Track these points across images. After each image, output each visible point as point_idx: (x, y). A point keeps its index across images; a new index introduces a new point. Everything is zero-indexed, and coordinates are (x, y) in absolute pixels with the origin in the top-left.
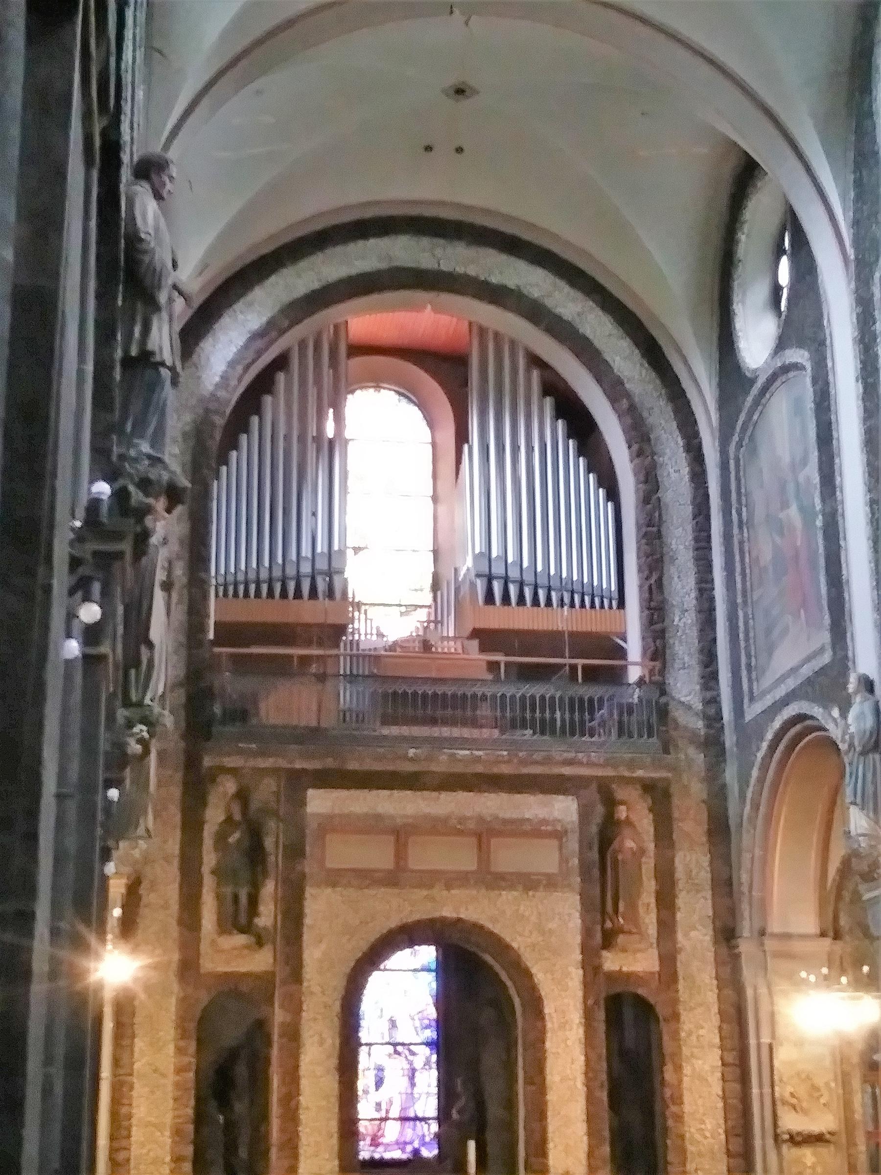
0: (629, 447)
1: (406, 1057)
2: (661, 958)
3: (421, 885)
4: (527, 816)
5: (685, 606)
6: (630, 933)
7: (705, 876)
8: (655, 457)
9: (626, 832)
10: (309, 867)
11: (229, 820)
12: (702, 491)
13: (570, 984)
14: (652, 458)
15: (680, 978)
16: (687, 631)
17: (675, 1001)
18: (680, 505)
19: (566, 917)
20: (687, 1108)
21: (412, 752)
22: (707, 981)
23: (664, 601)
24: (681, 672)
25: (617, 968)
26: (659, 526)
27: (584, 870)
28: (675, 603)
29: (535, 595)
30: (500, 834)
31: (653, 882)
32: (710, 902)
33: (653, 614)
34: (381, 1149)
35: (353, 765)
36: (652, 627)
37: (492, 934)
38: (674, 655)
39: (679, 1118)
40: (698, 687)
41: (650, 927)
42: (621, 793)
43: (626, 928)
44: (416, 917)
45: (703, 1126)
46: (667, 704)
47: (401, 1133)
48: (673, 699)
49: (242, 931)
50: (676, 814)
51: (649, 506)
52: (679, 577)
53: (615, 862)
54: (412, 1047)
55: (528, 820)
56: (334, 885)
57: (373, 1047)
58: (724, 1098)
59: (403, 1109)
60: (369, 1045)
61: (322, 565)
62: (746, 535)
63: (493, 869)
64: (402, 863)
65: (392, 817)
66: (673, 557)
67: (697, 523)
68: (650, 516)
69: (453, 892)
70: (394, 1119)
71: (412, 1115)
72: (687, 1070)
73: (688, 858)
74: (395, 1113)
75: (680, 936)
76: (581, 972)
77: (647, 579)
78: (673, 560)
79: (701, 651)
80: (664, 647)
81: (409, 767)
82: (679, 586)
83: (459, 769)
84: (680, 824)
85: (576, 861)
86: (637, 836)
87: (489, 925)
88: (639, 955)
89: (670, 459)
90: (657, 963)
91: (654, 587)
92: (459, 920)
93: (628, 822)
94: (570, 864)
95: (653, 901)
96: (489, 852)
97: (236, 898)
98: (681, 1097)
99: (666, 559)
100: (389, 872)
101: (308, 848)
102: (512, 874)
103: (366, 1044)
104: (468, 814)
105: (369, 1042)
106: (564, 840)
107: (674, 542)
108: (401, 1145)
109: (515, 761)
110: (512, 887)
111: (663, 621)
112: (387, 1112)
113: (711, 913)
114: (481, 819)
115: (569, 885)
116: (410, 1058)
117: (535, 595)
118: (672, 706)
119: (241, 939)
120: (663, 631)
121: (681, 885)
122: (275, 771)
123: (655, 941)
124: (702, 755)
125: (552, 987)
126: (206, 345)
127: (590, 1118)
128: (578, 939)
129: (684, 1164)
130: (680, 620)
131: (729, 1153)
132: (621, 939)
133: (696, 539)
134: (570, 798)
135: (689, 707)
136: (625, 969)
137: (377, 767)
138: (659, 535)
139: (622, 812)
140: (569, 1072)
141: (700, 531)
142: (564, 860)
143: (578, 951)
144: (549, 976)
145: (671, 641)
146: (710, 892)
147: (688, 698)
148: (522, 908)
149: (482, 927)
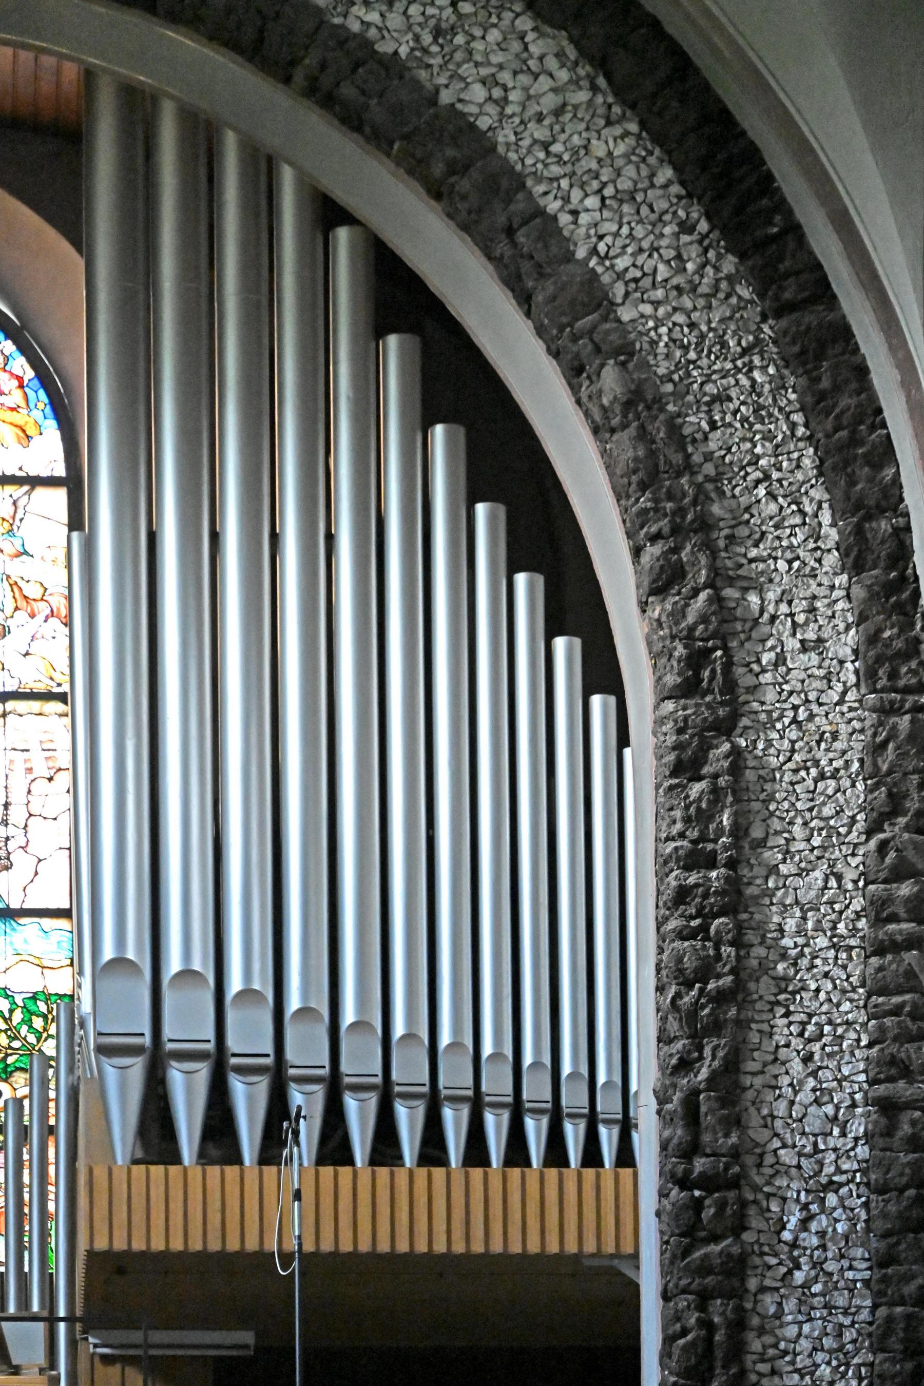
0: (637, 552)
5: (829, 1169)
8: (730, 593)
14: (717, 600)
16: (831, 1266)
18: (822, 776)
28: (787, 1157)
33: (698, 1205)
36: (697, 1254)
51: (696, 789)
52: (807, 1059)
66: (786, 979)
67: (883, 847)
77: (685, 1065)
80: (738, 1325)
82: (805, 1096)
89: (786, 597)
91: (705, 1102)
99: (764, 988)
107: (791, 925)
111: (739, 1227)
130: (804, 1224)
145: (769, 1303)
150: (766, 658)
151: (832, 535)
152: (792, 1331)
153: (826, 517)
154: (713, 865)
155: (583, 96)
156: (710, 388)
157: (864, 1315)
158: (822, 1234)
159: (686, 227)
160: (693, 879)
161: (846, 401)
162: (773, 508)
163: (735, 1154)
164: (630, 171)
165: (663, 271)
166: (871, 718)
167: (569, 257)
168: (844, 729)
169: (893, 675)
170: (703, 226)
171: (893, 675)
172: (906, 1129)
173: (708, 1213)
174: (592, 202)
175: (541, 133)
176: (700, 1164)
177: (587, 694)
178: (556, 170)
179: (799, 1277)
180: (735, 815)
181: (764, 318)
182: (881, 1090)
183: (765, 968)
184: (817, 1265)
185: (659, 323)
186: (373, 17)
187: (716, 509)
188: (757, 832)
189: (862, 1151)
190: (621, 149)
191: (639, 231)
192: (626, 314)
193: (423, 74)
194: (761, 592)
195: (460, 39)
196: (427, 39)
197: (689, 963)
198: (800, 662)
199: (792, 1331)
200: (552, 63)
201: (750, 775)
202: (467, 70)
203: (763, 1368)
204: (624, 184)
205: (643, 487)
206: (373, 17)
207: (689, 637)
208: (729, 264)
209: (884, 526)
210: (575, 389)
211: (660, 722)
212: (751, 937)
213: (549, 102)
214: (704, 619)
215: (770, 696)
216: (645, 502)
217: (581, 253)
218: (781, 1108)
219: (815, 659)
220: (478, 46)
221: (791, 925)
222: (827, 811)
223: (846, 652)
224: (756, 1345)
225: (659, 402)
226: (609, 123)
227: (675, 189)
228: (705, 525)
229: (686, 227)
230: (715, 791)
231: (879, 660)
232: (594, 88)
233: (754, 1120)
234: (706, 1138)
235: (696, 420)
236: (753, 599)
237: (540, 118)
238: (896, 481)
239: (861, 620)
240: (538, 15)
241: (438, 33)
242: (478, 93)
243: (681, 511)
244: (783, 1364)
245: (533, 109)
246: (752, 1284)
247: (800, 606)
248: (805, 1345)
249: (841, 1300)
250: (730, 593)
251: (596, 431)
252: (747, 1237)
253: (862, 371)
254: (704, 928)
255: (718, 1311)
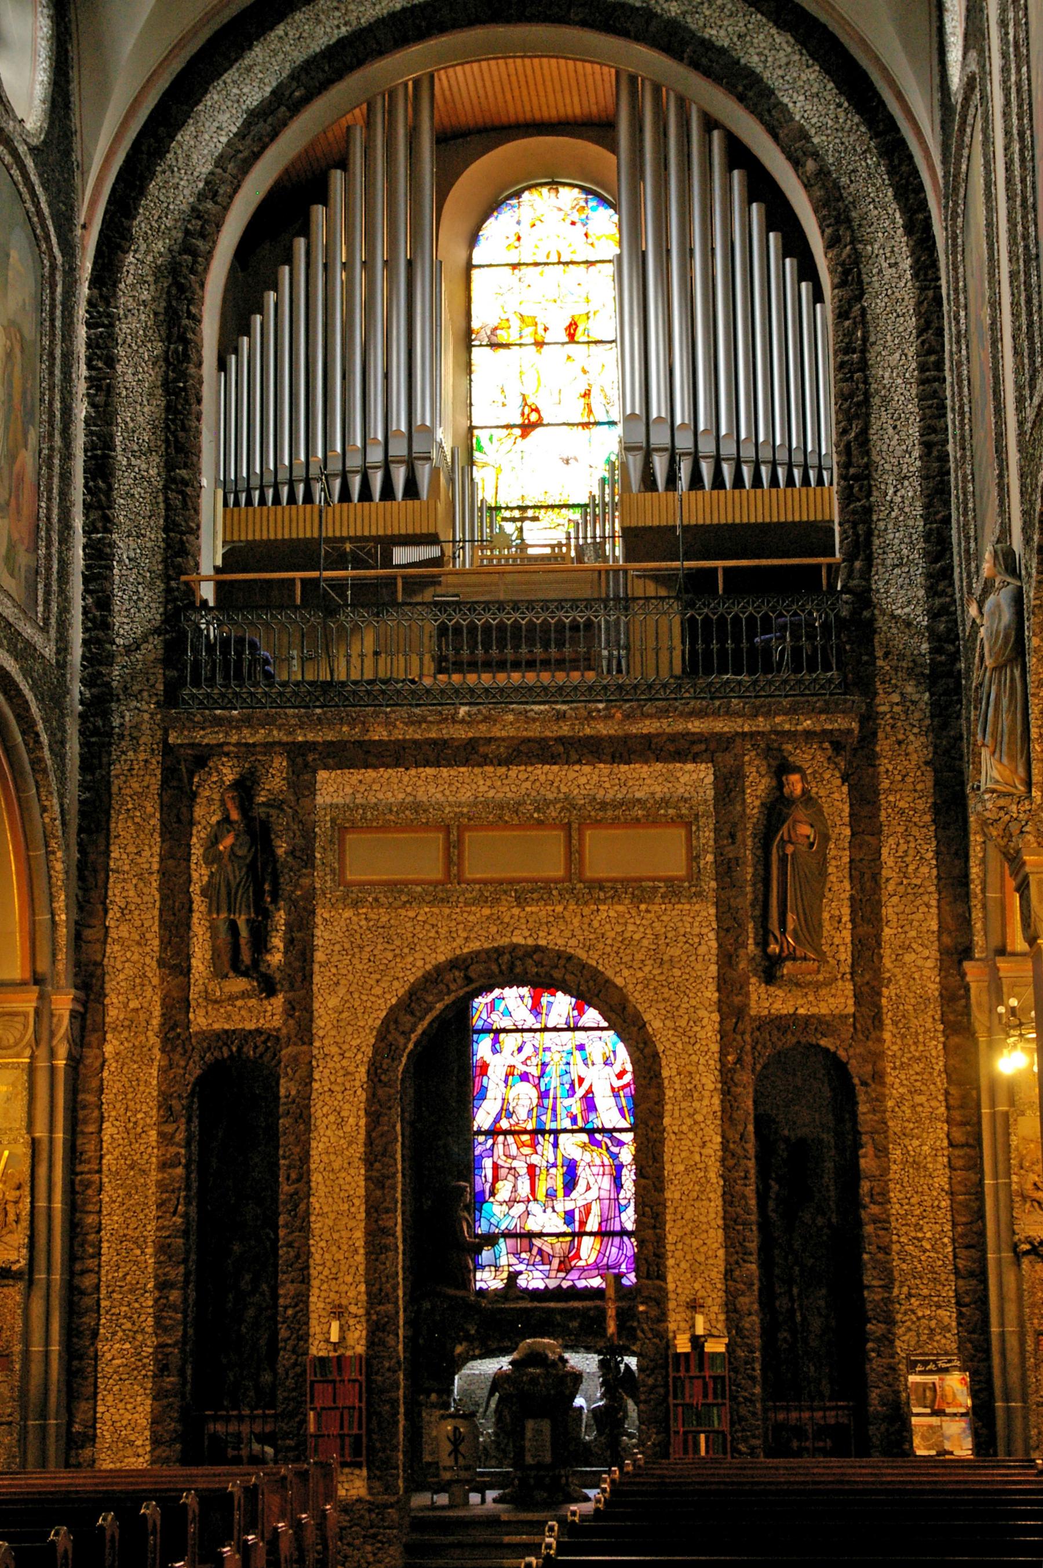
0: (823, 232)
1: (608, 1149)
2: (858, 997)
3: (481, 900)
4: (638, 795)
6: (805, 958)
7: (928, 872)
8: (860, 246)
9: (800, 812)
10: (321, 880)
11: (226, 820)
12: (930, 293)
13: (701, 1034)
15: (888, 1021)
16: (907, 510)
17: (880, 1055)
19: (697, 940)
20: (895, 1209)
21: (463, 710)
22: (929, 1025)
23: (867, 466)
24: (897, 571)
25: (791, 1012)
26: (864, 351)
27: (726, 869)
28: (887, 467)
29: (718, 473)
30: (598, 823)
31: (847, 885)
32: (934, 910)
33: (851, 487)
34: (574, 1275)
35: (379, 734)
37: (584, 966)
38: (885, 547)
39: (883, 1222)
40: (921, 593)
41: (842, 949)
42: (804, 756)
43: (799, 953)
44: (475, 946)
45: (920, 1235)
46: (873, 619)
47: (601, 1253)
48: (883, 613)
49: (245, 974)
50: (885, 784)
51: (847, 323)
52: (895, 427)
53: (783, 860)
54: (616, 1134)
55: (639, 800)
56: (355, 904)
57: (562, 1137)
58: (952, 1193)
59: (604, 1220)
60: (556, 1132)
61: (398, 449)
62: (964, 352)
63: (588, 874)
64: (454, 870)
65: (440, 807)
67: (923, 343)
68: (850, 334)
69: (528, 909)
70: (591, 1234)
71: (618, 1228)
72: (896, 1154)
73: (903, 847)
74: (592, 1225)
75: (887, 963)
76: (715, 1016)
78: (886, 401)
79: (927, 537)
80: (869, 533)
81: (460, 733)
82: (894, 442)
83: (535, 731)
84: (891, 798)
85: (710, 858)
86: (818, 819)
87: (582, 954)
88: (823, 992)
90: (851, 1002)
92: (537, 948)
93: (808, 799)
94: (702, 862)
95: (846, 911)
96: (581, 852)
97: (233, 927)
98: (884, 1193)
99: (876, 400)
100: (436, 883)
101: (318, 855)
102: (614, 880)
103: (551, 1132)
104: (550, 796)
105: (553, 1126)
106: (694, 828)
107: (887, 375)
108: (598, 1268)
109: (619, 715)
110: (616, 898)
111: (869, 494)
112: (583, 1224)
113: (935, 928)
114: (569, 804)
115: (699, 894)
116: (615, 1150)
117: (718, 473)
118: (881, 622)
119: (240, 984)
120: (868, 510)
121: (891, 887)
122: (269, 747)
123: (848, 970)
124: (927, 694)
125: (674, 1039)
126: (185, 136)
127: (730, 1223)
128: (714, 968)
129: (888, 1287)
130: (895, 493)
131: (957, 1272)
132: (787, 968)
133: (922, 368)
134: (703, 766)
135: (909, 625)
136: (801, 1011)
137: (413, 733)
138: (864, 365)
139: (795, 784)
140: (697, 1158)
141: (929, 352)
142: (693, 858)
143: (712, 987)
144: (669, 1023)
145: (881, 525)
146: (936, 896)
147: (907, 610)
148: (631, 928)
149: (570, 958)
150: (875, 271)
151: (900, 221)
152: (891, 536)
153: (898, 215)
154: (854, 352)
155: (797, 57)
156: (850, 167)
157: (921, 529)
158: (902, 497)
159: (839, 105)
160: (846, 358)
161: (904, 168)
162: (876, 212)
163: (867, 466)
164: (816, 85)
165: (830, 123)
166: (917, 292)
167: (792, 119)
168: (907, 297)
169: (926, 275)
170: (846, 104)
171: (926, 275)
172: (935, 453)
173: (856, 489)
174: (802, 98)
175: (780, 72)
176: (852, 471)
177: (799, 282)
178: (787, 86)
179: (893, 514)
180: (863, 333)
181: (871, 139)
182: (925, 438)
183: (877, 391)
184: (901, 509)
185: (829, 143)
186: (714, 32)
187: (853, 214)
188: (872, 339)
189: (918, 463)
190: (813, 76)
191: (820, 108)
192: (816, 140)
193: (734, 53)
194: (872, 244)
195: (748, 38)
196: (735, 39)
197: (846, 391)
198: (888, 272)
199: (891, 536)
200: (785, 46)
201: (869, 317)
202: (751, 50)
203: (880, 551)
204: (814, 90)
205: (824, 206)
206: (714, 32)
207: (843, 264)
208: (857, 119)
209: (921, 216)
210: (796, 171)
211: (833, 298)
212: (871, 380)
213: (784, 61)
214: (849, 256)
215: (876, 285)
216: (825, 212)
217: (797, 118)
218: (885, 448)
219: (894, 270)
220: (755, 41)
221: (887, 375)
222: (901, 329)
223: (907, 267)
224: (876, 542)
225: (829, 172)
226: (808, 67)
227: (835, 91)
228: (849, 220)
229: (839, 105)
230: (855, 323)
231: (919, 269)
232: (801, 54)
233: (874, 453)
234: (854, 460)
235: (844, 180)
236: (869, 248)
237: (780, 67)
238: (925, 199)
239: (912, 254)
240: (778, 27)
241: (739, 36)
242: (756, 58)
243: (839, 214)
244: (888, 550)
245: (777, 63)
246: (875, 518)
247: (888, 250)
248: (896, 541)
249: (911, 523)
250: (860, 246)
251: (805, 186)
252: (872, 499)
253: (910, 157)
254: (852, 377)
255: (861, 529)
